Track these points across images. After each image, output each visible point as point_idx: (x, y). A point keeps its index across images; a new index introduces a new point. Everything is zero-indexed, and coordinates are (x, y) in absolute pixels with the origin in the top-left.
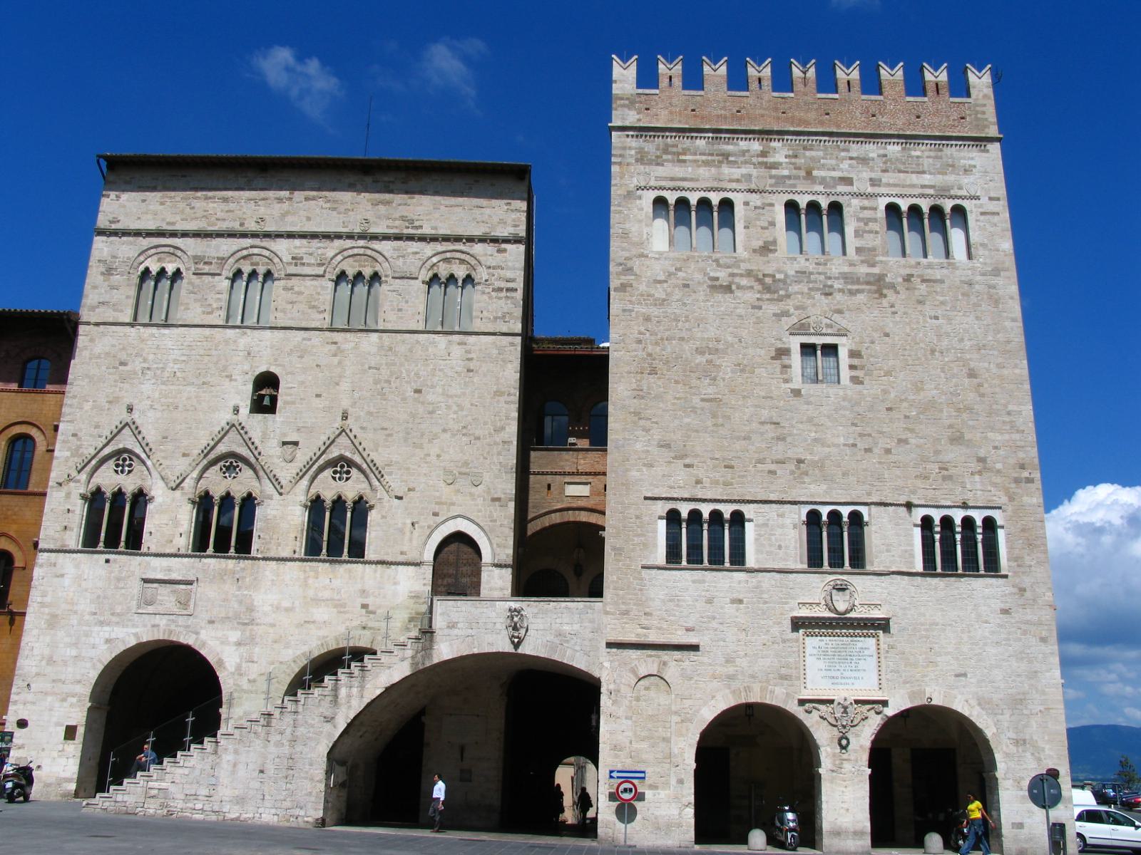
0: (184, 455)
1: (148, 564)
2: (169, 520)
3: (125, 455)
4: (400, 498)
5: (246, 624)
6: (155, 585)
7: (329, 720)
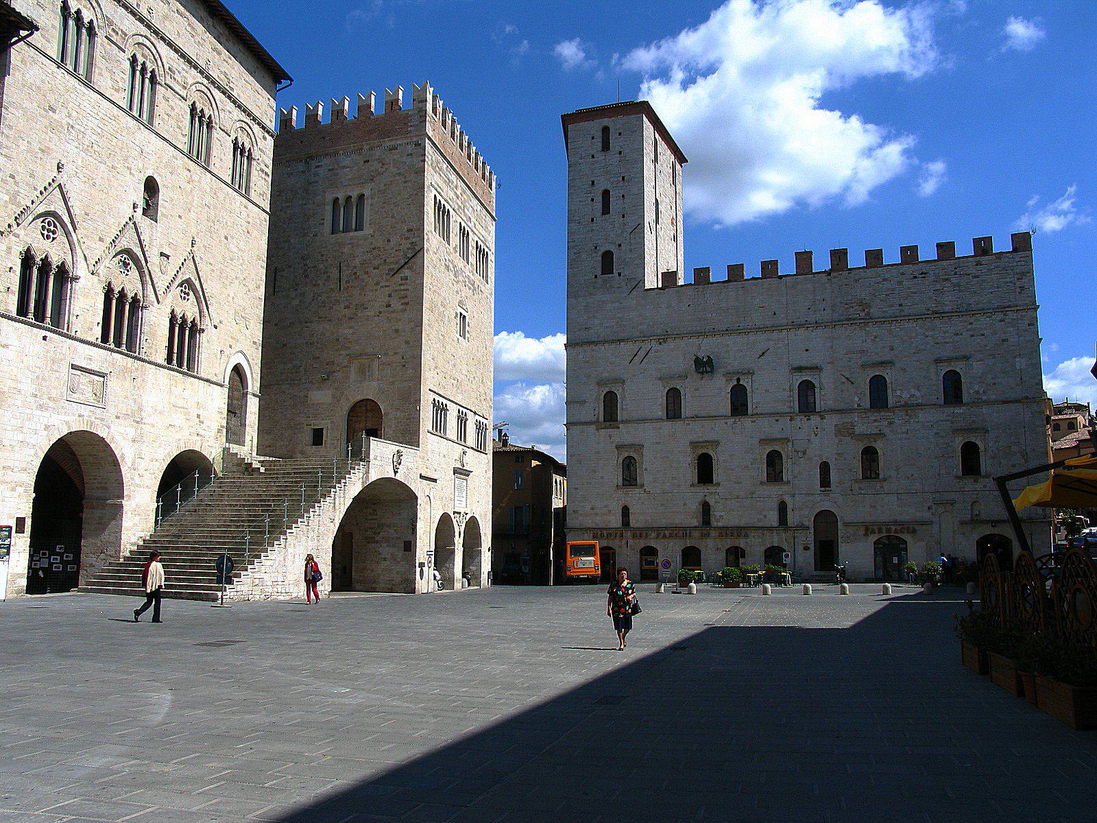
0: (101, 240)
1: (75, 349)
2: (85, 304)
3: (51, 219)
4: (216, 327)
5: (138, 422)
6: (78, 373)
7: (333, 521)
